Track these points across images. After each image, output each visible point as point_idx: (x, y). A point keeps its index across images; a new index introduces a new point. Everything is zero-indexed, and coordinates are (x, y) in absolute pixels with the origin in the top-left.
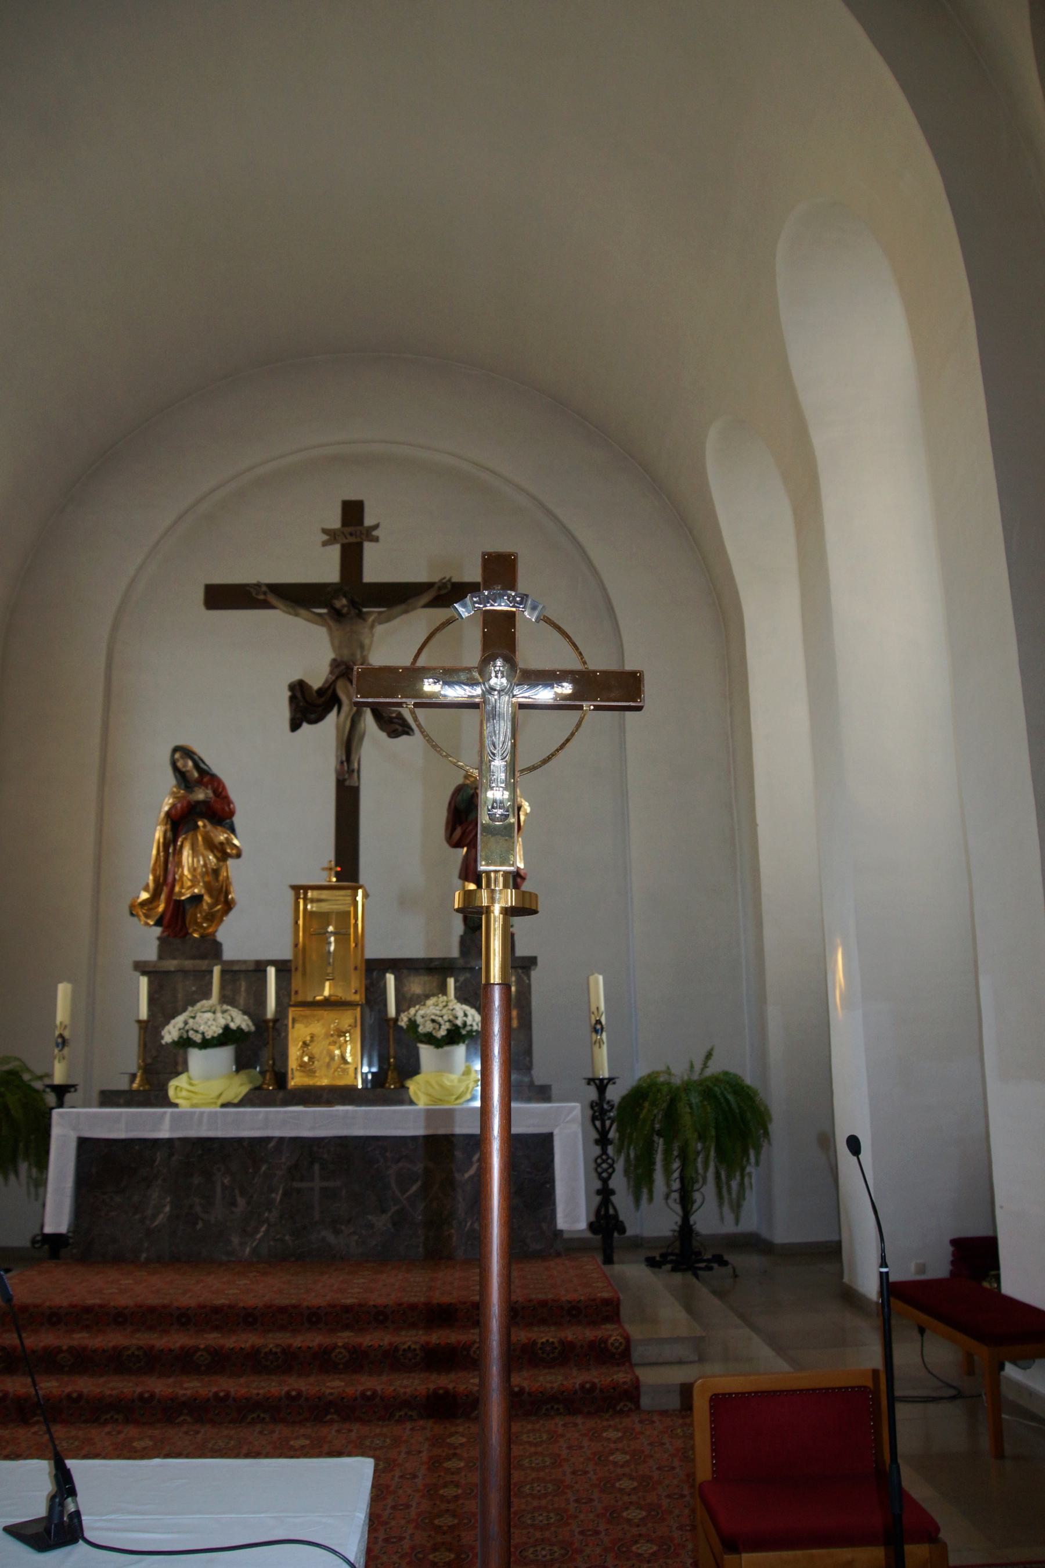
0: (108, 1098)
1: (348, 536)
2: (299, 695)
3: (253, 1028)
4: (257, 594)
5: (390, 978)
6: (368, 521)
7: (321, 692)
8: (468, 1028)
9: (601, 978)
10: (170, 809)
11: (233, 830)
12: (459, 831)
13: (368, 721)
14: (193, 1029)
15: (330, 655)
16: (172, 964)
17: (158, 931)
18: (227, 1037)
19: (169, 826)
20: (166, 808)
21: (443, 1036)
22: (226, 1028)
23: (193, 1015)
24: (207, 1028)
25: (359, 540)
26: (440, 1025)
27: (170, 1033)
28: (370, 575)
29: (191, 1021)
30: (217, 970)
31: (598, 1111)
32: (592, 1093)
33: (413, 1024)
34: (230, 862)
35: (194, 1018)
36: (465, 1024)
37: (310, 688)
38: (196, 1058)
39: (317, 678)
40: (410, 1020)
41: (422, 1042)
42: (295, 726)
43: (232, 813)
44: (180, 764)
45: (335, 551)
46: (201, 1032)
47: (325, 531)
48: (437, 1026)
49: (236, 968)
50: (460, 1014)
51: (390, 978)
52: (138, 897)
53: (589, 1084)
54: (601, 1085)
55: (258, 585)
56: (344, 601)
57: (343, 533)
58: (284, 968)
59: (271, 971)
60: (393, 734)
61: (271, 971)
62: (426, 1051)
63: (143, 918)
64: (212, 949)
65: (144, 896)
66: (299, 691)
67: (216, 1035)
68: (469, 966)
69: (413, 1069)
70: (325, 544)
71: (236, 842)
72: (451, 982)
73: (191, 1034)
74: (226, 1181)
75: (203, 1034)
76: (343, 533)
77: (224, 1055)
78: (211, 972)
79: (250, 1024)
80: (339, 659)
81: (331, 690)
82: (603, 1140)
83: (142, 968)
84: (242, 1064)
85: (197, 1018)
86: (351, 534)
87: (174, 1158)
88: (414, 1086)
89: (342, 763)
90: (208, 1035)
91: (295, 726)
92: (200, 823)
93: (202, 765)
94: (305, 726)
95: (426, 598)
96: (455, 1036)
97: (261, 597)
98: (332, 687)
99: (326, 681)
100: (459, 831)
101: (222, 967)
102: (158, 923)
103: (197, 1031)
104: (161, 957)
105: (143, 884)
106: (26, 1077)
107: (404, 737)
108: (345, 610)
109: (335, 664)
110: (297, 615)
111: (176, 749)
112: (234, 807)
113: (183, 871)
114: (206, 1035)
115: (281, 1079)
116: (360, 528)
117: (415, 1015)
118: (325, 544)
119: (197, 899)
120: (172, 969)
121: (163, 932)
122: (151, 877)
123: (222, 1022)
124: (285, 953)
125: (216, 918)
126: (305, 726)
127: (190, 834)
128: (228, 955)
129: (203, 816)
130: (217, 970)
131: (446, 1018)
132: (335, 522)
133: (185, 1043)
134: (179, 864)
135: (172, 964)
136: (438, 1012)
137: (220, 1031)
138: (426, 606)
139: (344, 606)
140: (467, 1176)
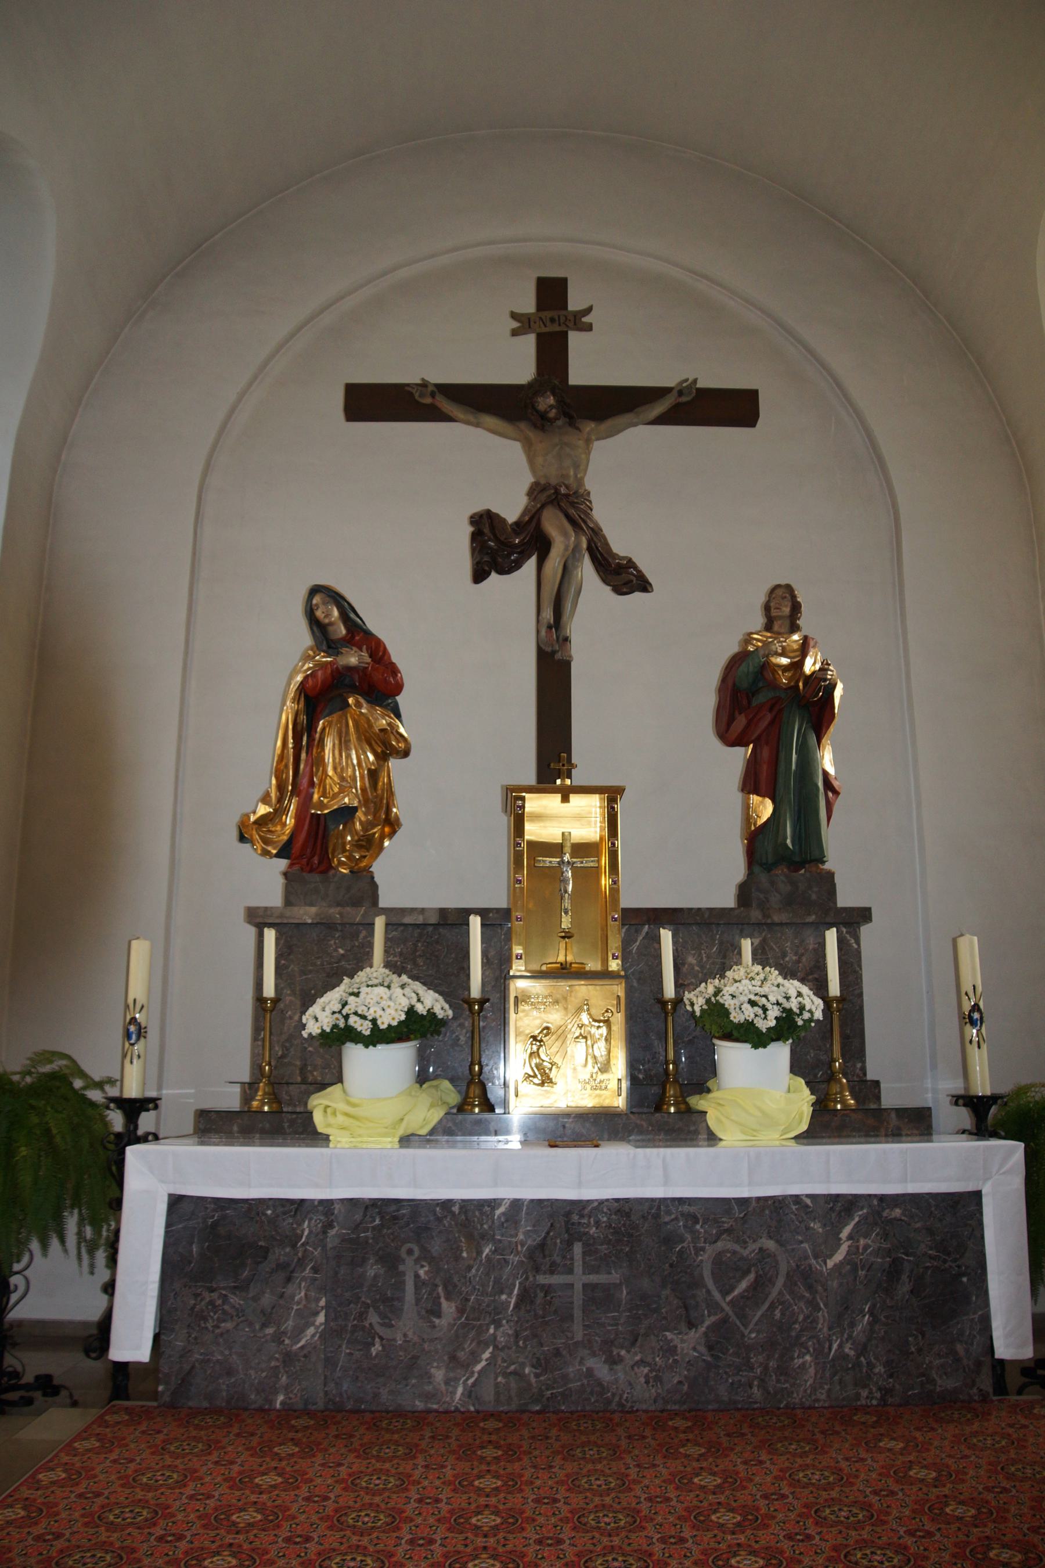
1: (548, 323)
2: (486, 530)
3: (450, 1013)
4: (422, 395)
5: (666, 936)
6: (574, 304)
8: (806, 1016)
10: (306, 678)
11: (398, 716)
12: (741, 721)
13: (587, 571)
14: (356, 1013)
15: (527, 479)
17: (283, 864)
19: (302, 705)
21: (769, 1029)
22: (411, 1012)
23: (356, 990)
24: (380, 1012)
25: (563, 328)
26: (765, 1009)
29: (352, 999)
30: (380, 923)
33: (717, 1010)
34: (393, 763)
35: (357, 995)
36: (802, 1008)
37: (504, 521)
40: (708, 1001)
41: (728, 1037)
42: (479, 576)
43: (398, 688)
44: (319, 614)
45: (529, 342)
46: (370, 1018)
47: (514, 316)
48: (760, 1011)
49: (407, 920)
50: (793, 993)
51: (666, 936)
52: (254, 812)
53: (956, 1104)
55: (424, 385)
56: (551, 400)
57: (541, 318)
59: (475, 923)
61: (475, 923)
63: (259, 845)
65: (263, 810)
67: (395, 1023)
68: (769, 921)
70: (515, 333)
71: (402, 730)
73: (353, 1021)
74: (421, 1272)
75: (374, 1021)
76: (541, 318)
78: (372, 925)
79: (447, 1006)
80: (543, 481)
81: (533, 524)
83: (258, 919)
85: (362, 995)
86: (552, 320)
87: (332, 1232)
89: (550, 627)
90: (383, 1023)
91: (479, 576)
92: (351, 700)
93: (352, 615)
94: (494, 575)
95: (659, 408)
97: (428, 400)
98: (533, 524)
99: (526, 511)
100: (741, 721)
101: (387, 918)
102: (283, 852)
103: (364, 1017)
104: (288, 902)
105: (260, 794)
106: (78, 1084)
107: (637, 595)
108: (552, 414)
109: (535, 491)
110: (477, 425)
111: (315, 590)
112: (401, 678)
113: (325, 772)
114: (379, 1022)
116: (563, 312)
117: (716, 994)
118: (515, 333)
119: (347, 813)
120: (309, 921)
121: (291, 865)
122: (274, 781)
123: (405, 1003)
125: (370, 845)
126: (494, 578)
127: (335, 717)
129: (355, 690)
130: (380, 923)
131: (772, 999)
132: (528, 304)
134: (320, 761)
135: (307, 914)
136: (758, 990)
137: (403, 1017)
138: (660, 420)
139: (551, 407)
140: (830, 1263)
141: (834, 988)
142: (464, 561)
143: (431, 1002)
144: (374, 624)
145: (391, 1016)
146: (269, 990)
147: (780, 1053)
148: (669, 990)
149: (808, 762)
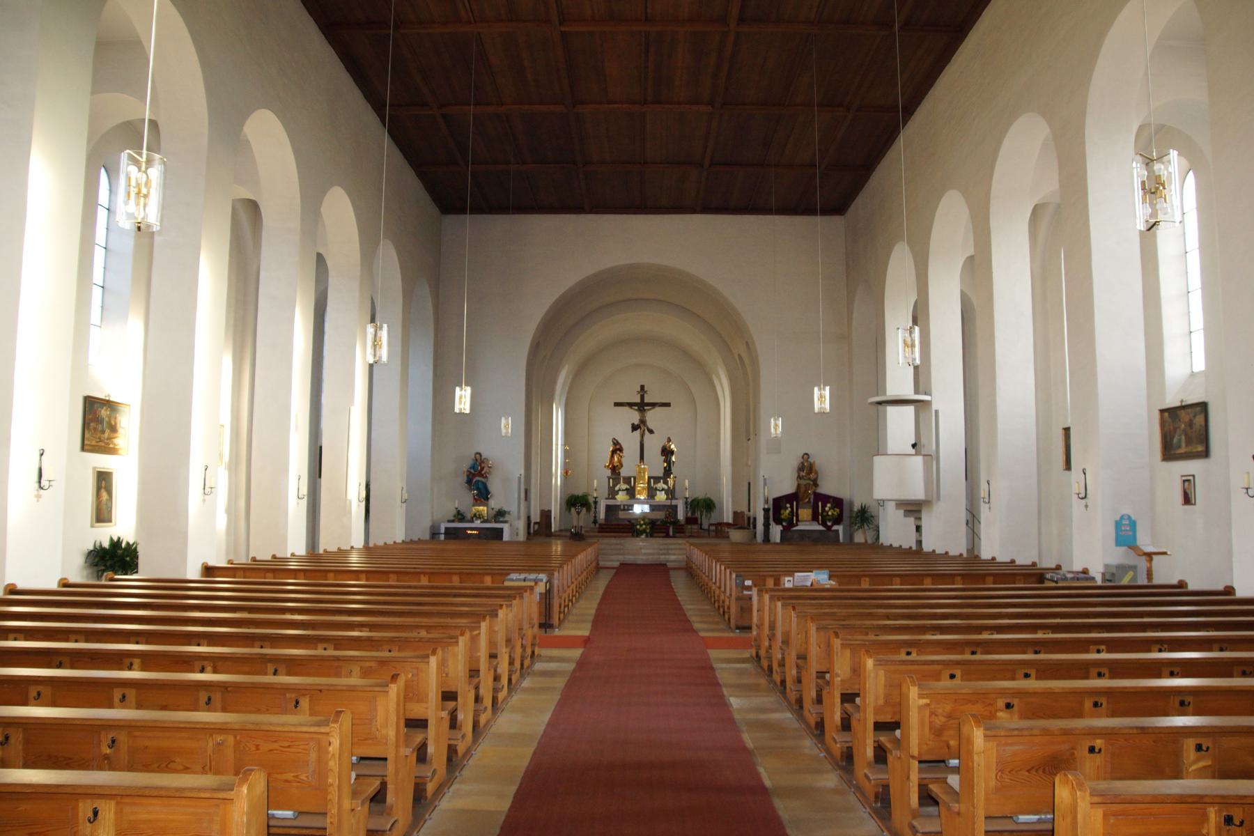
6: (645, 390)
9: (687, 481)
13: (646, 431)
16: (614, 477)
18: (626, 489)
20: (611, 449)
27: (617, 488)
28: (646, 400)
31: (686, 503)
33: (656, 488)
38: (620, 493)
39: (636, 422)
42: (633, 432)
45: (639, 396)
54: (687, 498)
58: (635, 478)
59: (632, 479)
60: (651, 433)
61: (632, 479)
62: (658, 492)
64: (619, 474)
66: (633, 425)
72: (662, 481)
77: (625, 492)
82: (687, 508)
84: (627, 494)
88: (656, 498)
91: (633, 432)
96: (663, 490)
125: (620, 469)
132: (639, 390)
133: (620, 490)
135: (614, 477)
143: (628, 487)
144: (620, 442)
145: (624, 488)
146: (611, 485)
147: (663, 492)
148: (652, 485)
149: (670, 459)
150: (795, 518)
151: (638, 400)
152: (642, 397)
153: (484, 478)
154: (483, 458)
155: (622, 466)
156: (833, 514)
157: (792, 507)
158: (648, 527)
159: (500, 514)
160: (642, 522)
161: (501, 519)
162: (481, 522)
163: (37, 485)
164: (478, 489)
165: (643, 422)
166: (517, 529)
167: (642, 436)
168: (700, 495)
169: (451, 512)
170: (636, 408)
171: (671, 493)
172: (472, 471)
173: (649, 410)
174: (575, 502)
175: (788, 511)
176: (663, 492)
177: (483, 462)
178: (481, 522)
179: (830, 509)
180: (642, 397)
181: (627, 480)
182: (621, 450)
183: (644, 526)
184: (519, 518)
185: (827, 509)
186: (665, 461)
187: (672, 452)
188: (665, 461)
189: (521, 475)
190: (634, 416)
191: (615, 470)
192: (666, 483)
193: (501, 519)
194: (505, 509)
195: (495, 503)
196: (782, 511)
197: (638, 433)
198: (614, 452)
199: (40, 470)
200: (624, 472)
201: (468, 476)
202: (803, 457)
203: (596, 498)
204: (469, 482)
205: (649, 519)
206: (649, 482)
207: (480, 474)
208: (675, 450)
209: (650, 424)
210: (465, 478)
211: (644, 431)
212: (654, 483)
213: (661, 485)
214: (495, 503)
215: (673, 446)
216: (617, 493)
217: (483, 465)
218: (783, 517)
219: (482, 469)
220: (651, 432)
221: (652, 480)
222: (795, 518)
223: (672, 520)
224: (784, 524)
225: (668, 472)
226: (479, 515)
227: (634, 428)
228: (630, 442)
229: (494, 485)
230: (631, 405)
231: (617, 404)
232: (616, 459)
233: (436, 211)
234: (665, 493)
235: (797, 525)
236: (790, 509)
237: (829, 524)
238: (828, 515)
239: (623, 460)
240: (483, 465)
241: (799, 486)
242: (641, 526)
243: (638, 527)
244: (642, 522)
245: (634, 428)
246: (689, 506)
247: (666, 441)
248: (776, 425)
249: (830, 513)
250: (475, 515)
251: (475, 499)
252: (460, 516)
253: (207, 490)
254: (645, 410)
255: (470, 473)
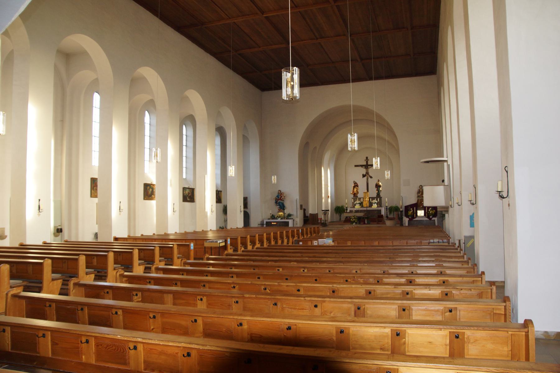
0: (351, 208)
7: (365, 175)
9: (387, 199)
13: (369, 177)
16: (354, 198)
18: (359, 203)
27: (355, 203)
31: (387, 209)
32: (386, 207)
38: (357, 205)
39: (365, 174)
42: (363, 178)
54: (387, 207)
58: (363, 198)
59: (362, 199)
62: (373, 204)
64: (357, 197)
66: (363, 175)
69: (372, 205)
72: (375, 199)
77: (359, 204)
83: (352, 198)
84: (360, 205)
88: (372, 207)
91: (363, 178)
96: (375, 203)
115: (363, 206)
124: (363, 197)
125: (357, 194)
128: (358, 197)
132: (365, 159)
133: (356, 204)
135: (354, 198)
141: (378, 201)
142: (362, 177)
144: (357, 182)
147: (376, 204)
149: (379, 189)
150: (415, 215)
151: (365, 164)
152: (367, 162)
153: (282, 201)
154: (282, 192)
155: (358, 193)
156: (432, 213)
157: (413, 210)
158: (356, 220)
159: (289, 215)
160: (353, 218)
161: (290, 218)
162: (281, 219)
163: (38, 211)
164: (280, 205)
165: (367, 173)
166: (297, 222)
167: (367, 179)
168: (394, 205)
169: (269, 216)
170: (364, 167)
171: (380, 204)
172: (277, 198)
173: (370, 168)
174: (339, 210)
175: (411, 212)
176: (376, 204)
177: (282, 194)
178: (281, 219)
179: (431, 210)
180: (367, 162)
181: (360, 199)
182: (357, 186)
183: (354, 220)
184: (297, 217)
185: (429, 210)
186: (377, 190)
187: (380, 186)
188: (377, 190)
189: (297, 199)
190: (363, 171)
191: (355, 195)
192: (377, 200)
193: (290, 218)
194: (291, 213)
195: (287, 211)
196: (409, 212)
197: (365, 178)
198: (354, 187)
199: (39, 206)
200: (359, 195)
201: (276, 201)
202: (419, 187)
203: (347, 207)
204: (276, 202)
205: (357, 216)
206: (370, 200)
207: (280, 199)
208: (382, 185)
209: (370, 174)
210: (274, 201)
211: (368, 177)
212: (372, 200)
213: (375, 201)
214: (287, 211)
215: (380, 183)
216: (355, 205)
217: (281, 195)
218: (409, 214)
219: (281, 197)
220: (371, 177)
221: (371, 199)
222: (415, 215)
223: (366, 216)
224: (410, 218)
225: (378, 195)
226: (279, 216)
227: (364, 176)
228: (362, 183)
229: (287, 204)
230: (362, 166)
231: (356, 166)
232: (355, 190)
233: (257, 91)
234: (377, 204)
235: (416, 217)
236: (412, 211)
237: (431, 217)
238: (430, 213)
239: (359, 190)
240: (281, 195)
241: (418, 200)
242: (353, 219)
243: (351, 220)
244: (353, 218)
245: (364, 176)
246: (388, 210)
247: (377, 181)
248: (388, 174)
249: (431, 212)
250: (278, 216)
251: (279, 209)
252: (273, 217)
253: (121, 210)
254: (368, 168)
255: (277, 199)
